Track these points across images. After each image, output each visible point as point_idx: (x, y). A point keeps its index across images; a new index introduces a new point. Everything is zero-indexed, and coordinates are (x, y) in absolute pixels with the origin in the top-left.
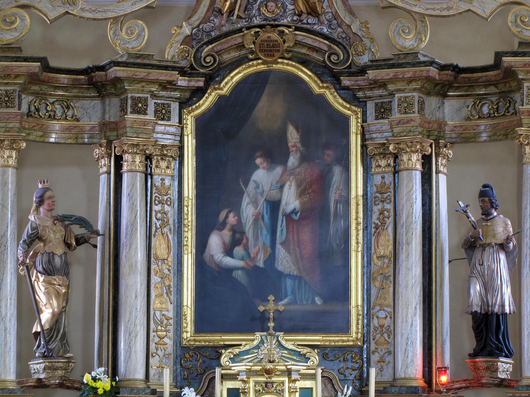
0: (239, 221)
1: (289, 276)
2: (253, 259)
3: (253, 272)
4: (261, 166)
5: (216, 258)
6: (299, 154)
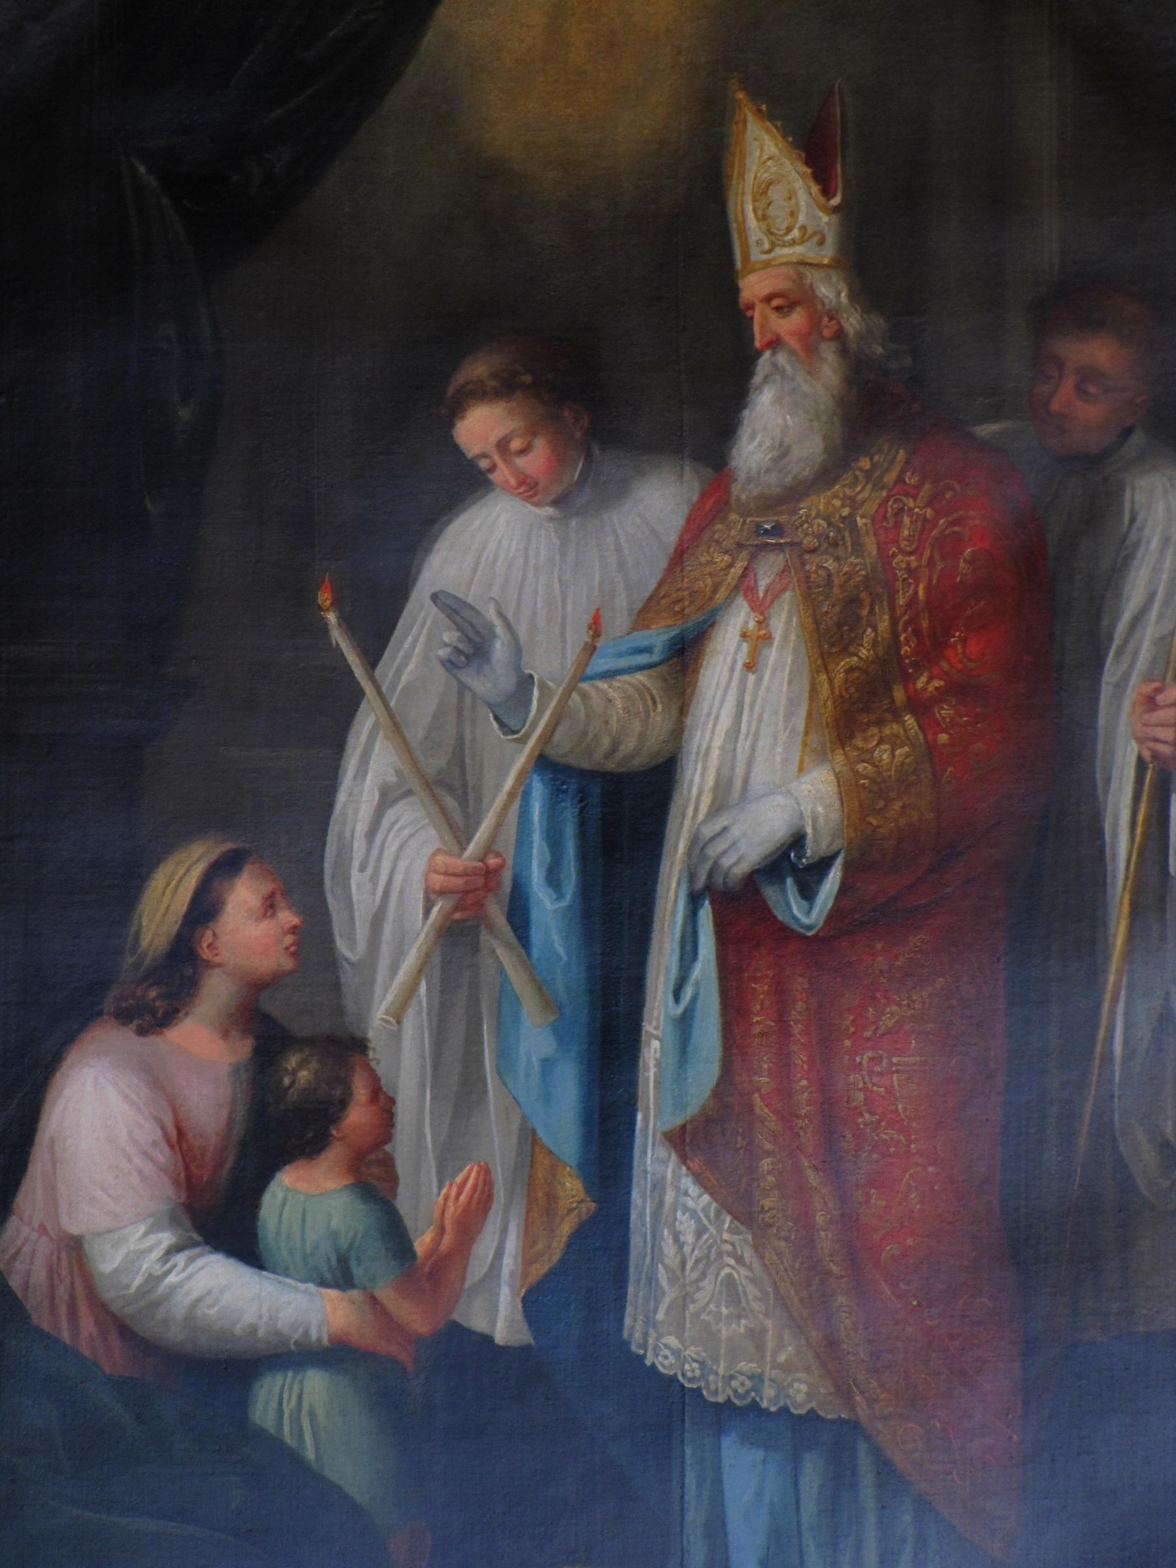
0: (314, 941)
1: (741, 1415)
2: (434, 1276)
3: (437, 1389)
4: (502, 474)
5: (108, 1261)
6: (830, 370)
